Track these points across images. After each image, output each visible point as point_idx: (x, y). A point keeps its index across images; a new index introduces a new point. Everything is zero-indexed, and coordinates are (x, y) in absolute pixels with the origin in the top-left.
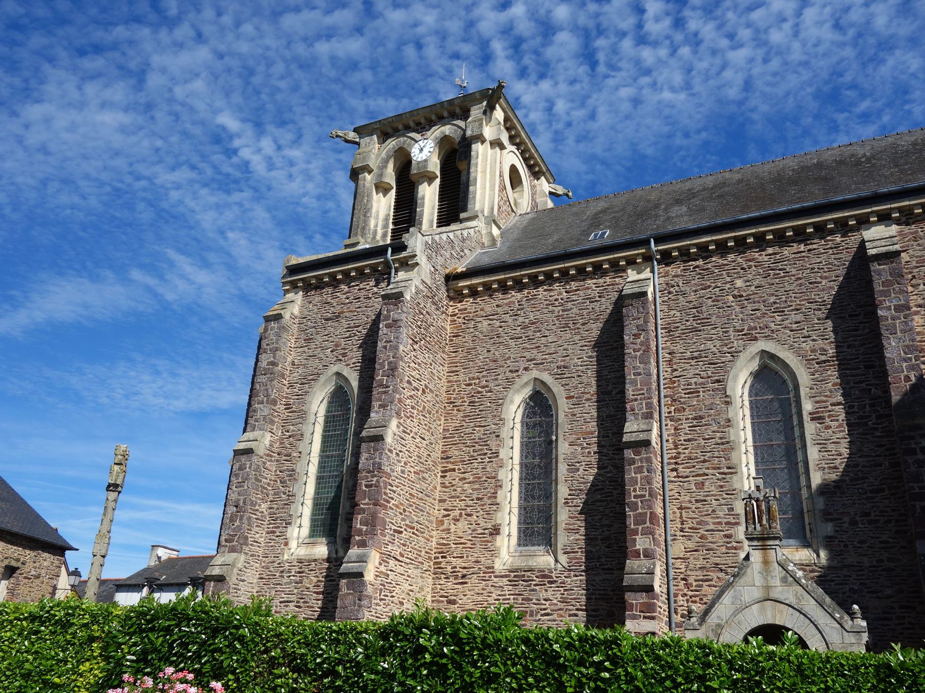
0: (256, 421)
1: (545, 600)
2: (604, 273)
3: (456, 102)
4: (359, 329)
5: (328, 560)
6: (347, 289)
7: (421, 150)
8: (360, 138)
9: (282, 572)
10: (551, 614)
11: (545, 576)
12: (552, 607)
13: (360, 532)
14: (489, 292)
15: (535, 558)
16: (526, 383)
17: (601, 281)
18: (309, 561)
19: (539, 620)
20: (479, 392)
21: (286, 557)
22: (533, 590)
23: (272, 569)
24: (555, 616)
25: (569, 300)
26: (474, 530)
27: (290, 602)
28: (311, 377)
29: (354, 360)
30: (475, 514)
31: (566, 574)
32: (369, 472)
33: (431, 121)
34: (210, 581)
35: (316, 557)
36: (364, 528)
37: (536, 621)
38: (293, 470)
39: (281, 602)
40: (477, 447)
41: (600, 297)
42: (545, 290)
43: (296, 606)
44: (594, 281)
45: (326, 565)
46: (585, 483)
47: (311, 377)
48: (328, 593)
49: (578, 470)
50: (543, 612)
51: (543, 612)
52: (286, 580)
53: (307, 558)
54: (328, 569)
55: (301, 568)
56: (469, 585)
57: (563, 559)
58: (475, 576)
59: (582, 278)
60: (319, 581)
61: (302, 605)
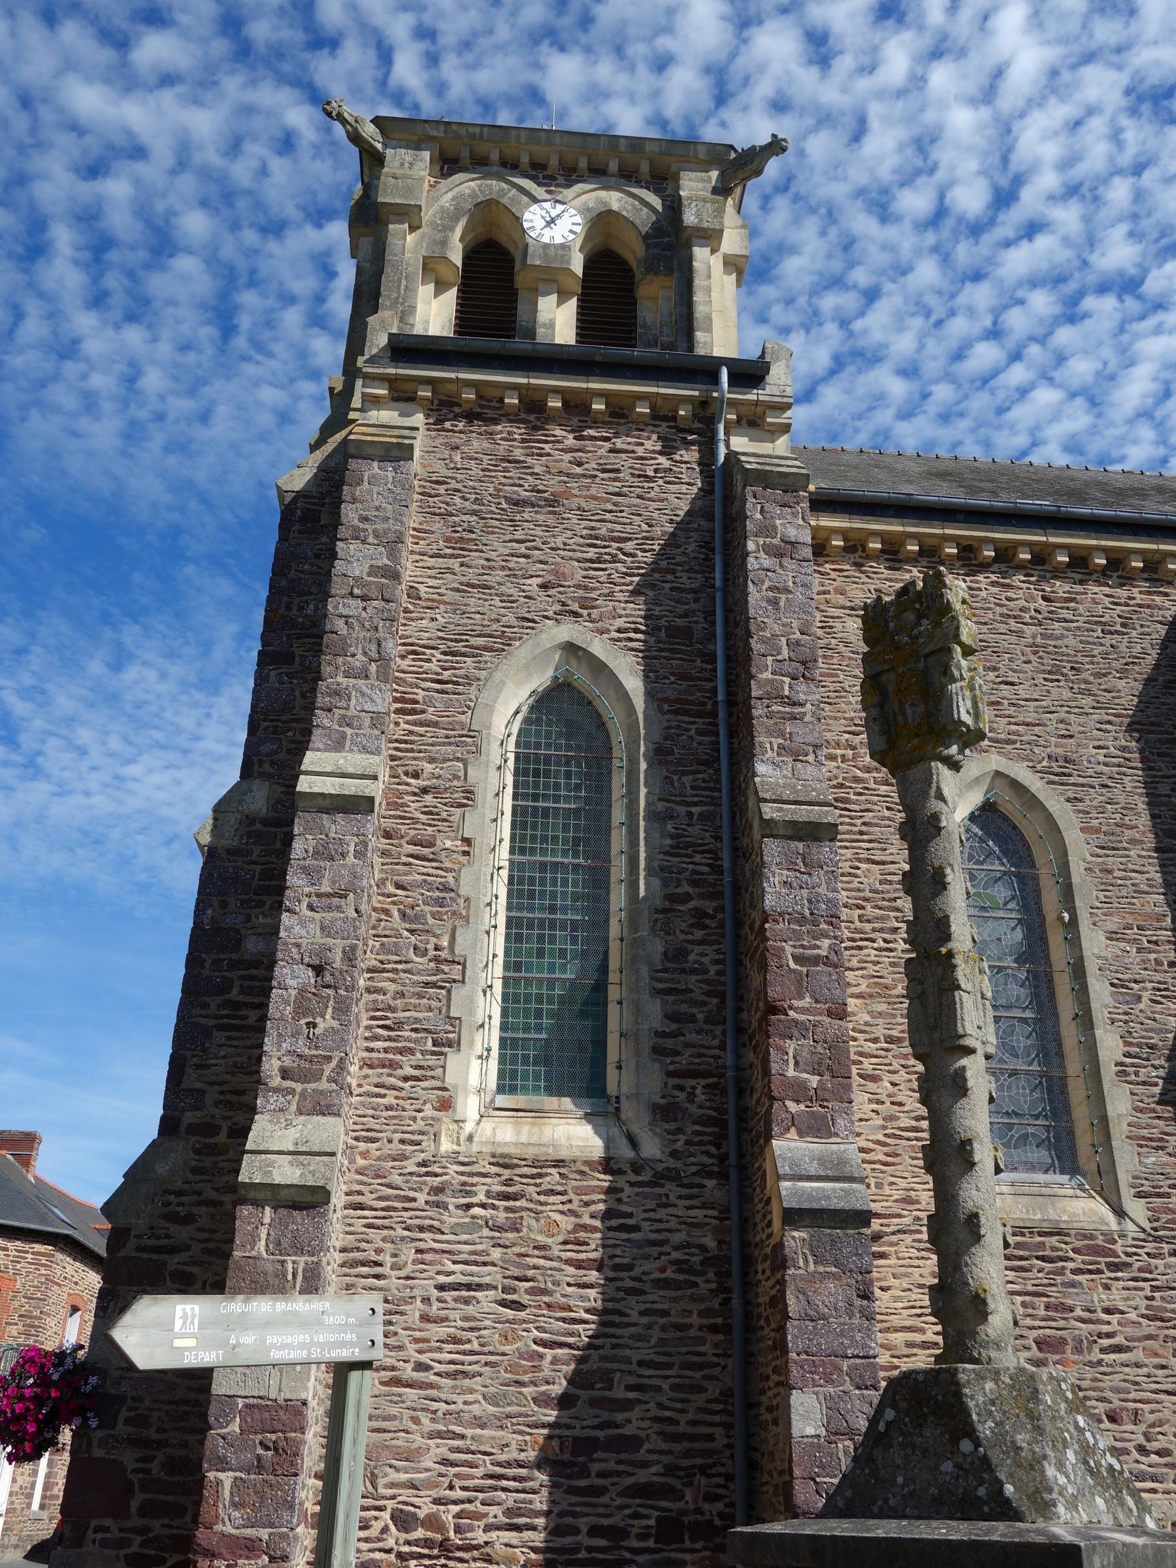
0: (347, 722)
1: (1108, 1311)
2: (1127, 579)
3: (649, 147)
4: (629, 546)
5: (607, 1165)
6: (570, 441)
7: (551, 222)
8: (385, 145)
9: (439, 1190)
10: (1128, 1349)
11: (1099, 1253)
12: (1129, 1331)
13: (799, 1092)
14: (856, 557)
15: (1061, 1203)
16: (977, 780)
17: (1123, 593)
18: (536, 1163)
19: (1100, 1362)
20: (857, 780)
21: (446, 1146)
22: (1073, 1284)
23: (396, 1179)
24: (1138, 1355)
25: (1052, 617)
26: (891, 1118)
27: (479, 1287)
28: (481, 641)
29: (620, 623)
30: (887, 1078)
31: (1150, 1247)
32: (802, 921)
33: (574, 170)
34: (258, 1204)
35: (563, 1154)
36: (814, 1081)
37: (1091, 1364)
38: (446, 888)
39: (441, 1288)
40: (870, 911)
41: (1123, 625)
42: (993, 584)
43: (503, 1303)
44: (1107, 590)
45: (605, 1180)
46: (1160, 1031)
47: (481, 641)
48: (617, 1267)
49: (1139, 999)
50: (1106, 1342)
51: (1106, 1342)
52: (454, 1217)
53: (530, 1153)
54: (609, 1191)
55: (508, 1182)
56: (892, 1261)
57: (1137, 1209)
58: (908, 1238)
59: (1078, 577)
60: (584, 1227)
61: (525, 1299)
